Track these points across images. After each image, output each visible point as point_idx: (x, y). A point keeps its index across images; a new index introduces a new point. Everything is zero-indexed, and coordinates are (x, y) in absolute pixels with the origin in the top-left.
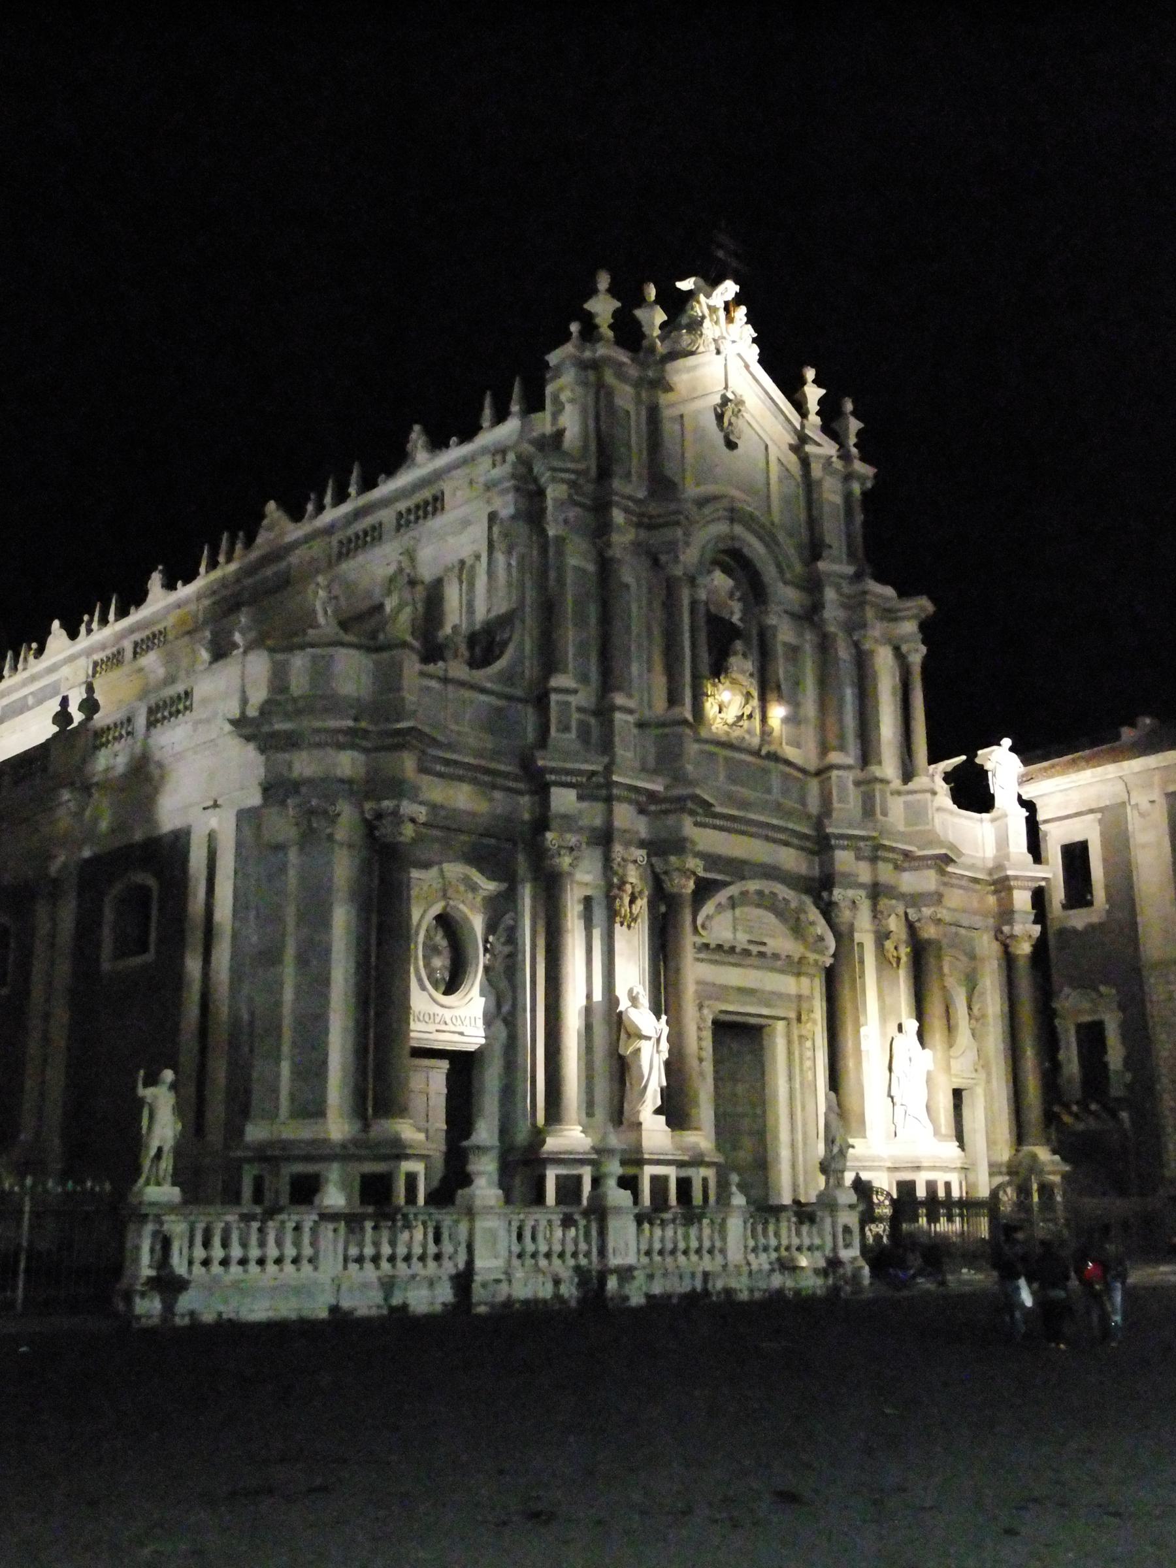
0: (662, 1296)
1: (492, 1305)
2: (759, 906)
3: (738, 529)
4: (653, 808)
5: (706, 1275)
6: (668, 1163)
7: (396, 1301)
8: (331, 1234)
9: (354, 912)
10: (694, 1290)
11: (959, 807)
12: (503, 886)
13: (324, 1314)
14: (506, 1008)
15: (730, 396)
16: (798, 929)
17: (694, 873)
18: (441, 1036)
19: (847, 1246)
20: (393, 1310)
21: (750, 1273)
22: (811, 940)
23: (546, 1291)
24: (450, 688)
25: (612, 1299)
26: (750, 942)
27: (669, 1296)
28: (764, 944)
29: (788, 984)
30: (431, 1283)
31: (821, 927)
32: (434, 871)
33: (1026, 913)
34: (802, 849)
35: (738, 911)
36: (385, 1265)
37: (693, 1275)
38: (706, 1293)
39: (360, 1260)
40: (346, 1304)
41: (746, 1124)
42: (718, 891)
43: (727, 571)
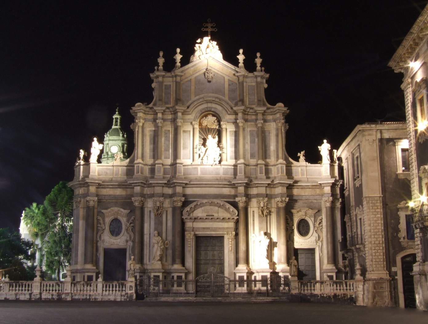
0: (77, 299)
1: (35, 299)
2: (210, 206)
3: (210, 105)
4: (172, 186)
5: (90, 295)
6: (159, 272)
7: (18, 297)
8: (7, 286)
9: (85, 222)
10: (86, 298)
11: (311, 163)
12: (129, 211)
13: (3, 299)
14: (132, 238)
15: (209, 68)
16: (227, 210)
17: (181, 201)
18: (112, 246)
19: (130, 290)
20: (16, 299)
21: (102, 295)
22: (231, 212)
23: (50, 297)
24: (114, 167)
25: (63, 298)
26: (207, 216)
27: (79, 299)
28: (213, 216)
29: (225, 225)
30: (25, 294)
31: (232, 208)
32: (109, 210)
33: (329, 194)
34: (231, 188)
35: (203, 208)
36: (17, 291)
37: (86, 295)
38: (90, 299)
39: (12, 290)
40: (8, 297)
41: (217, 262)
42: (190, 204)
43: (213, 116)
